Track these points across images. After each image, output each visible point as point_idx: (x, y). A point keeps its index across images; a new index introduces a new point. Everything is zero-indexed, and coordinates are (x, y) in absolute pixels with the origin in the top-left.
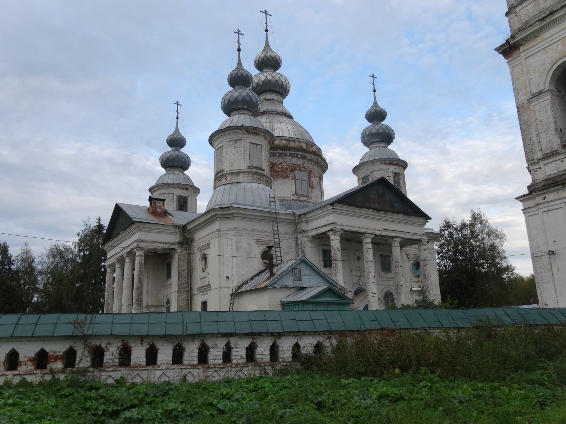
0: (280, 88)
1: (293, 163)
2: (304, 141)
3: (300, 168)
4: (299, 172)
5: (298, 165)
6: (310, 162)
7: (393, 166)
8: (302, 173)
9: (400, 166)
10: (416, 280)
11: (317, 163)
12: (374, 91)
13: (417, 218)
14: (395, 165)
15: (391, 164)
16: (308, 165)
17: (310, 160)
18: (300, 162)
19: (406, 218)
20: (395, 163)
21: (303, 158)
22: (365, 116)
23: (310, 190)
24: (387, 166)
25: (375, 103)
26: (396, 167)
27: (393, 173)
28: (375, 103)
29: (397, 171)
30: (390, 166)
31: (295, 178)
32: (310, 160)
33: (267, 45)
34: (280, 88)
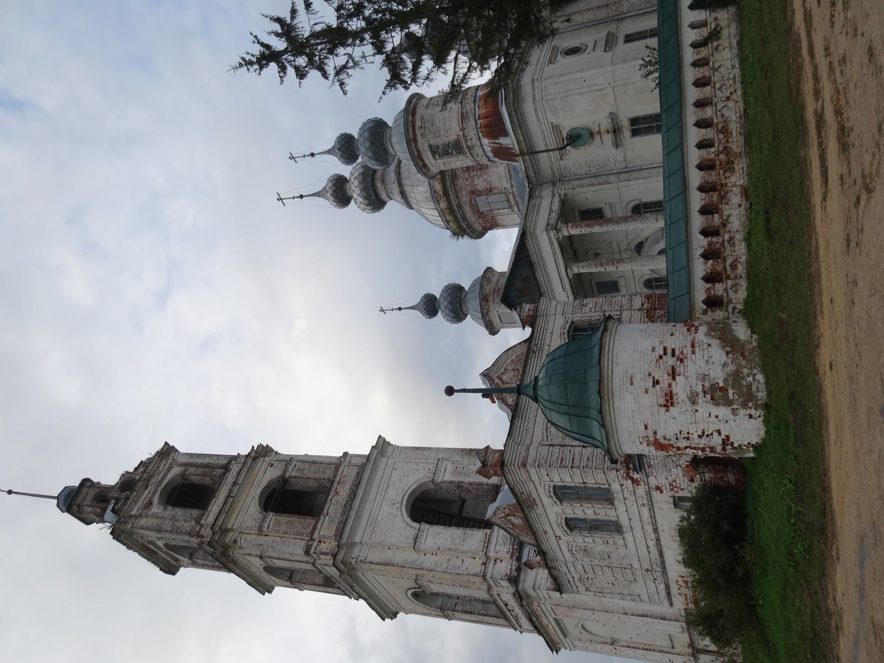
0: (370, 196)
3: (475, 208)
4: (480, 206)
5: (472, 209)
6: (459, 195)
7: (426, 161)
8: (479, 203)
9: (418, 151)
10: (597, 138)
11: (453, 181)
12: (313, 155)
13: (531, 253)
14: (422, 160)
15: (425, 165)
16: (465, 199)
18: (467, 209)
19: (537, 266)
21: (460, 206)
22: (382, 211)
23: (496, 191)
24: (431, 167)
25: (329, 152)
26: (424, 156)
27: (435, 158)
28: (329, 152)
29: (429, 153)
30: (428, 164)
32: (457, 197)
33: (317, 194)
34: (370, 196)
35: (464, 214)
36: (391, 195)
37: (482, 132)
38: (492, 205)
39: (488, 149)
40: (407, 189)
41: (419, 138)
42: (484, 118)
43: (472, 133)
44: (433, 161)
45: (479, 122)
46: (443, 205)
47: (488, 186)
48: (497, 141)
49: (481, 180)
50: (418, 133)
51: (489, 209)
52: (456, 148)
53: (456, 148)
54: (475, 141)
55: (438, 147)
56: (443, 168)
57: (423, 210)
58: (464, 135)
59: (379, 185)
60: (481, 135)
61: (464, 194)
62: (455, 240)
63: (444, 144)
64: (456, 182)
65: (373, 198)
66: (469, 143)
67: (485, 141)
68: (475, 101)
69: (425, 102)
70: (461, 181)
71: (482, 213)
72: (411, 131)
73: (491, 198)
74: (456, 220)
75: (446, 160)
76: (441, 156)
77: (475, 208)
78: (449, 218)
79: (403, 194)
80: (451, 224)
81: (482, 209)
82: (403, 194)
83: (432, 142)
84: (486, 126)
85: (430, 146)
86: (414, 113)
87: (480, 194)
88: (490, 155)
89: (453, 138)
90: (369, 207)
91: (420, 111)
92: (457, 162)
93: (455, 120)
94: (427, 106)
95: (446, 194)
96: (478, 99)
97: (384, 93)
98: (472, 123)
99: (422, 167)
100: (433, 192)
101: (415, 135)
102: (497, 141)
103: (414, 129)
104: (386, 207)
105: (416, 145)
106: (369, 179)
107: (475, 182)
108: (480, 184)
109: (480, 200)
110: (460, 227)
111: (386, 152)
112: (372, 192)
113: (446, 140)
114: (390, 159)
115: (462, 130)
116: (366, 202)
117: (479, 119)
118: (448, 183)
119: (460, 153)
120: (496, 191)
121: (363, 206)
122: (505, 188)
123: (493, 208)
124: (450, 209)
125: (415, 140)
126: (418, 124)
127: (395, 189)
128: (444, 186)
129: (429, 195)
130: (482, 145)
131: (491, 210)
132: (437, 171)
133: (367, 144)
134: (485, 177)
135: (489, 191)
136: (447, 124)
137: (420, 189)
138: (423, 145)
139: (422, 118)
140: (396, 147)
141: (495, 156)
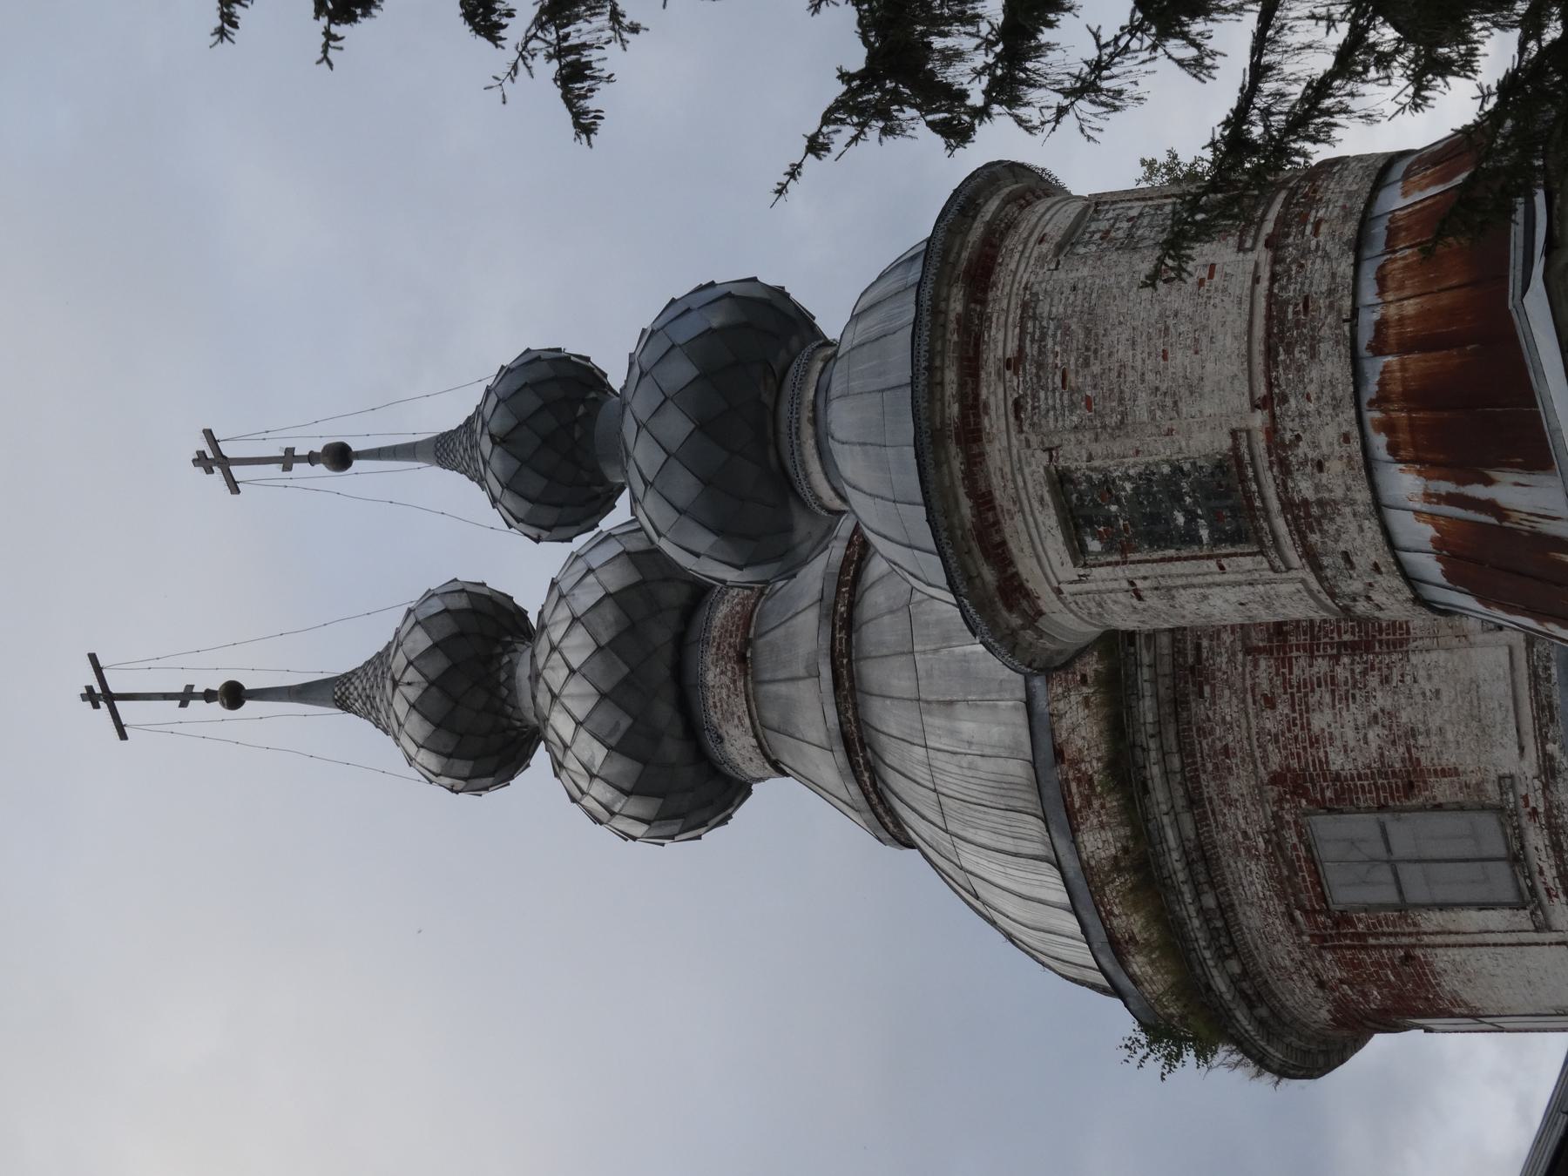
1: (1279, 926)
2: (1063, 846)
3: (1301, 882)
5: (1284, 886)
6: (1210, 789)
7: (1026, 567)
8: (1328, 852)
9: (984, 501)
11: (1178, 703)
14: (1000, 556)
15: (1013, 590)
16: (1242, 816)
17: (1194, 801)
18: (1251, 881)
20: (989, 575)
21: (1203, 858)
24: (1048, 601)
25: (442, 450)
26: (1016, 535)
27: (1078, 553)
28: (442, 450)
29: (1049, 519)
31: (1403, 908)
32: (1194, 801)
33: (332, 692)
35: (1226, 909)
36: (785, 750)
37: (1388, 427)
38: (1409, 873)
39: (1415, 532)
40: (889, 719)
41: (996, 421)
42: (1404, 348)
43: (1325, 431)
44: (1069, 571)
45: (1374, 368)
46: (1100, 843)
47: (1395, 756)
48: (1477, 491)
49: (1355, 714)
50: (995, 394)
51: (1390, 895)
52: (1218, 505)
53: (1218, 505)
54: (1339, 479)
55: (1107, 487)
56: (1124, 620)
57: (970, 858)
58: (1272, 431)
59: (715, 677)
60: (1379, 441)
61: (1238, 785)
62: (1154, 1066)
63: (1147, 476)
64: (1199, 710)
65: (673, 749)
66: (1304, 487)
67: (1404, 484)
68: (1359, 245)
69: (1059, 221)
70: (1228, 707)
71: (1343, 919)
72: (951, 375)
73: (1407, 833)
74: (1173, 944)
75: (1144, 571)
76: (1120, 547)
77: (1301, 882)
78: (1131, 923)
79: (859, 750)
80: (1138, 965)
81: (1343, 895)
82: (859, 750)
83: (1074, 457)
84: (1417, 397)
85: (1060, 481)
86: (981, 276)
87: (1343, 796)
88: (1429, 567)
89: (1204, 442)
90: (635, 806)
91: (1019, 269)
92: (1217, 594)
93: (1229, 343)
94: (1067, 244)
95: (1124, 770)
96: (1380, 231)
97: (816, 146)
98: (1332, 367)
99: (994, 597)
100: (1047, 751)
101: (972, 406)
102: (1477, 491)
103: (971, 367)
104: (744, 814)
105: (974, 461)
106: (661, 635)
107: (1319, 721)
108: (1347, 736)
109: (1340, 836)
110: (1192, 988)
111: (785, 486)
112: (664, 712)
113: (1161, 452)
114: (803, 526)
115: (1265, 403)
116: (623, 767)
117: (1378, 348)
118: (1147, 709)
119: (1237, 537)
120: (1443, 790)
121: (600, 790)
122: (1506, 782)
123: (1416, 893)
124: (1142, 867)
125: (971, 434)
126: (1000, 341)
127: (811, 710)
128: (1119, 728)
129: (1018, 770)
130: (1378, 506)
131: (1403, 908)
132: (1092, 631)
133: (677, 426)
134: (1382, 700)
135: (1402, 785)
136: (1180, 359)
137: (969, 726)
138: (1016, 467)
139: (1028, 309)
140: (851, 464)
141: (1456, 577)
